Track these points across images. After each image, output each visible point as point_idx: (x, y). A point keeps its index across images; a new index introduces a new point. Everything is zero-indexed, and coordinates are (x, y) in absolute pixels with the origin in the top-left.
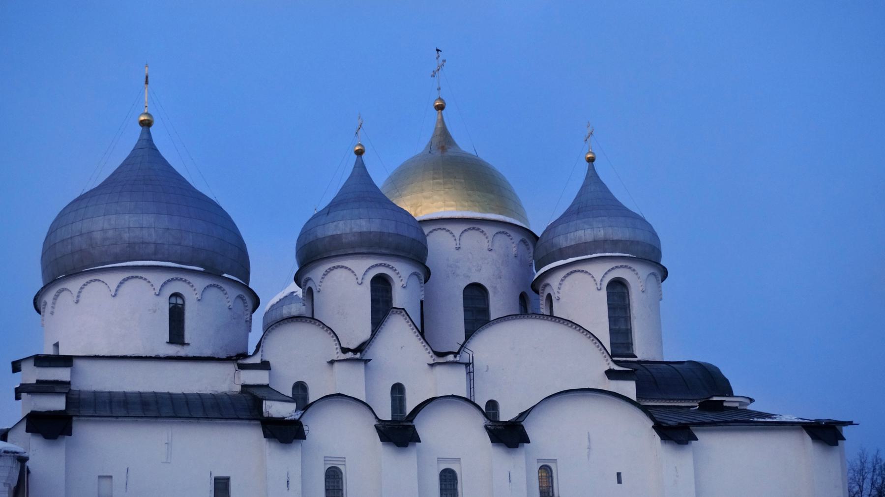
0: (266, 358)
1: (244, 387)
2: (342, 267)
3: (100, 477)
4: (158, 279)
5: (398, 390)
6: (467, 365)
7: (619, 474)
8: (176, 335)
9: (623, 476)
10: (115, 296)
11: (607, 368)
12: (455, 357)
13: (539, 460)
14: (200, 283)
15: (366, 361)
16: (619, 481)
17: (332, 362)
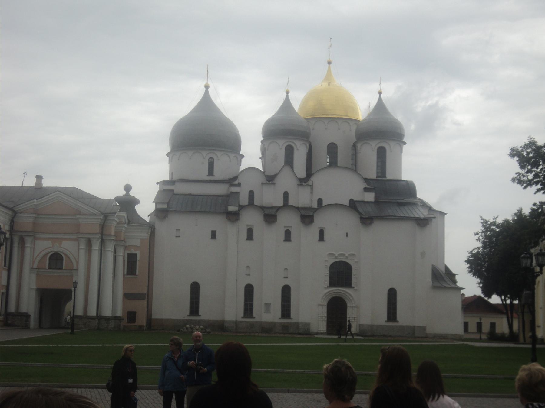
0: (239, 182)
1: (232, 193)
2: (276, 142)
3: (177, 230)
4: (204, 153)
5: (286, 195)
6: (310, 185)
7: (347, 234)
8: (211, 172)
9: (345, 235)
10: (190, 158)
11: (365, 187)
12: (305, 183)
13: (319, 228)
14: (219, 154)
15: (274, 184)
16: (347, 236)
17: (262, 184)
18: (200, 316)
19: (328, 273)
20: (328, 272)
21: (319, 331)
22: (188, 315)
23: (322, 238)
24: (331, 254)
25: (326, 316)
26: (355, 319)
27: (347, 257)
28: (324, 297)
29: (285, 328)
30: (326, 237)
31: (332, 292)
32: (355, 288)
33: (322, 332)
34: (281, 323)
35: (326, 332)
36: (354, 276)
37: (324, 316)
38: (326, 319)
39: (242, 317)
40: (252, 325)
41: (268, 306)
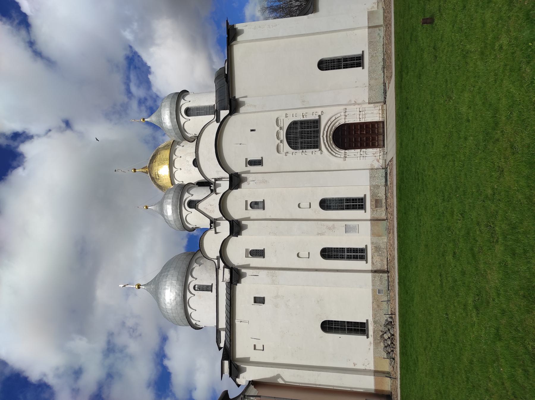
18: (367, 320)
19: (302, 152)
20: (301, 151)
21: (381, 158)
22: (368, 337)
23: (258, 163)
24: (278, 151)
25: (359, 150)
26: (360, 111)
27: (281, 128)
28: (334, 154)
29: (377, 203)
30: (257, 157)
31: (326, 143)
32: (320, 114)
33: (381, 154)
34: (373, 210)
35: (381, 149)
36: (305, 116)
37: (359, 153)
38: (364, 150)
39: (367, 263)
40: (377, 249)
41: (348, 230)
